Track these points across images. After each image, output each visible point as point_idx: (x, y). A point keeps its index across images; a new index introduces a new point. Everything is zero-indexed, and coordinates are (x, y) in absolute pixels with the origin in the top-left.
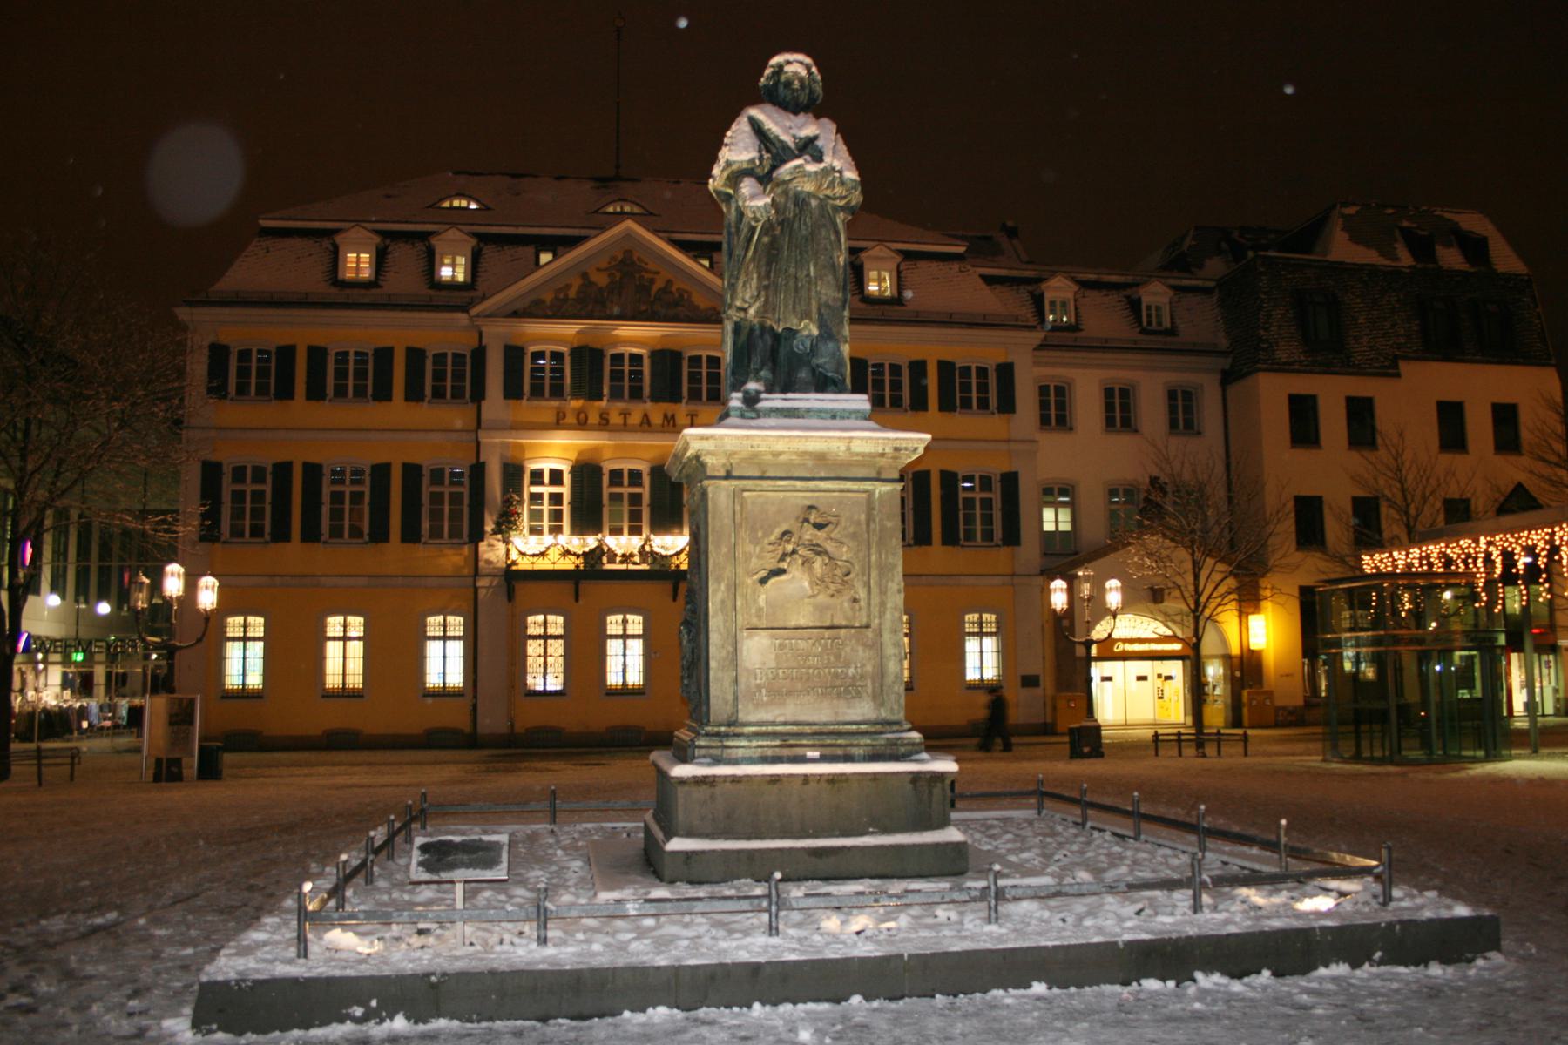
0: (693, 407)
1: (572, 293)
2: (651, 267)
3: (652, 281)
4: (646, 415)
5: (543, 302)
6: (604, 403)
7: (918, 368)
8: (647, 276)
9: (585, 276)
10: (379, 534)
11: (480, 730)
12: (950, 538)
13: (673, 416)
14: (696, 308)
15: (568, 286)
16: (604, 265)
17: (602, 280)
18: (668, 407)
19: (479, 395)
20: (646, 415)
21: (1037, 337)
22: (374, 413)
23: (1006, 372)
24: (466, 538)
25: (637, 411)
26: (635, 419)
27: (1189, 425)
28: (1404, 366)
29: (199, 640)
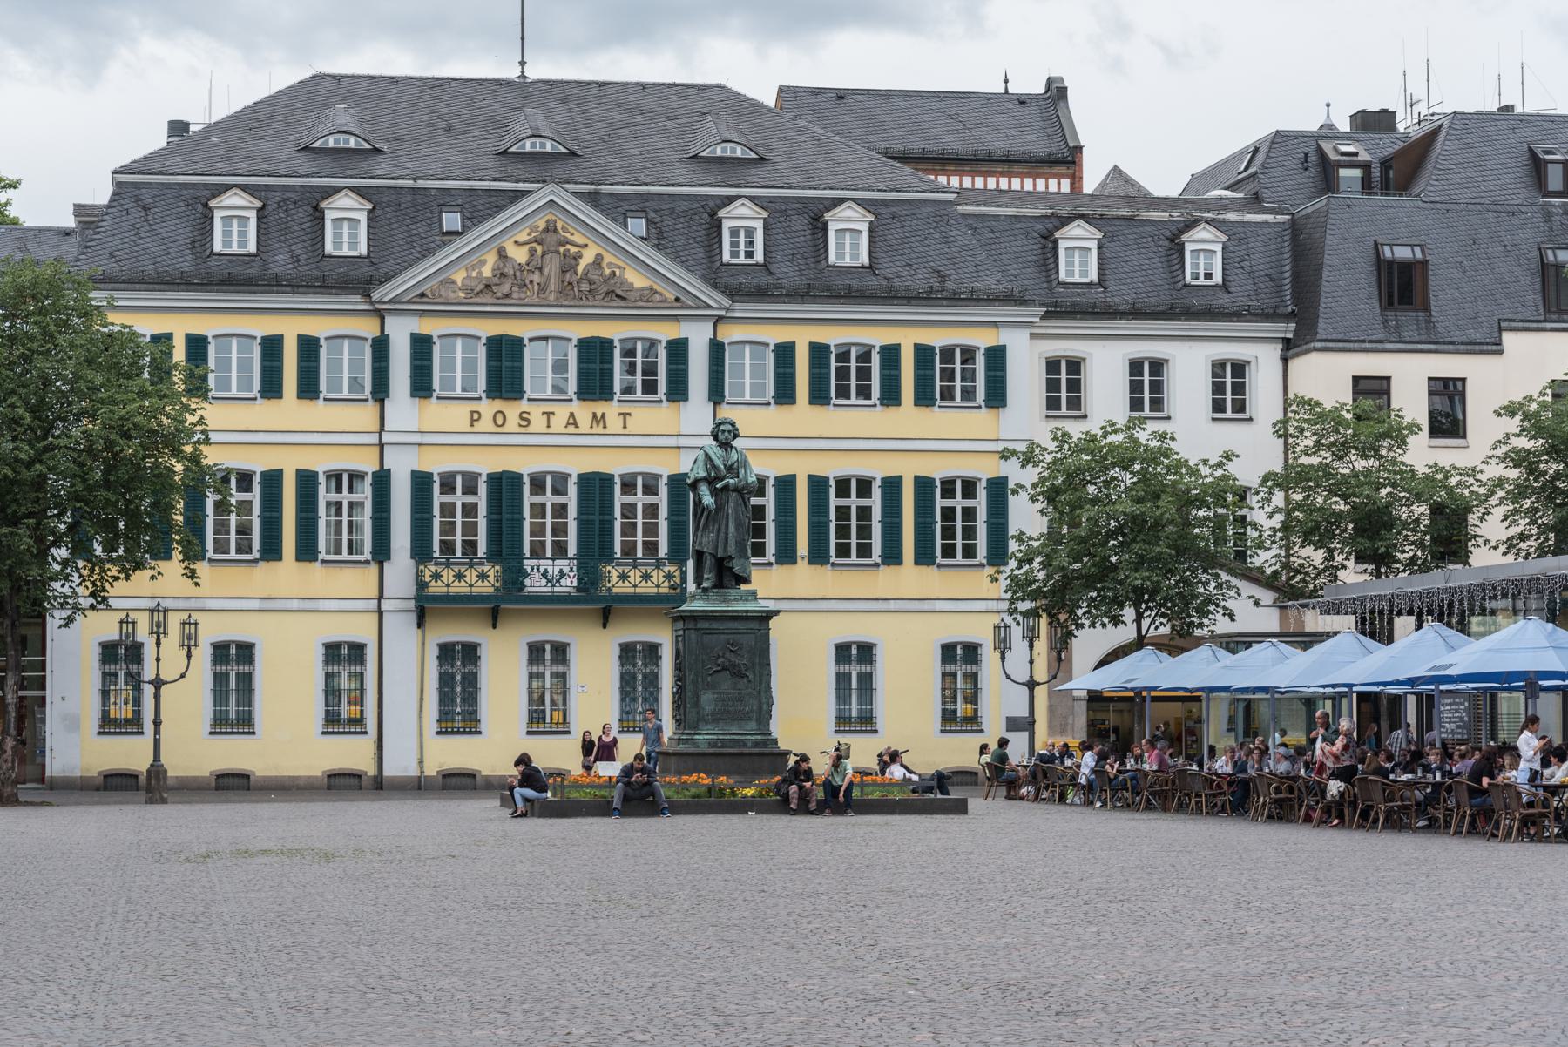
0: (626, 408)
1: (487, 271)
4: (572, 414)
5: (454, 282)
6: (524, 405)
7: (891, 354)
8: (573, 249)
9: (502, 254)
10: (271, 550)
11: (387, 772)
12: (924, 556)
13: (603, 415)
14: (631, 288)
15: (483, 262)
16: (523, 237)
17: (520, 255)
18: (600, 407)
19: (381, 390)
20: (572, 414)
21: (1034, 314)
22: (266, 414)
23: (996, 357)
24: (367, 555)
25: (561, 413)
26: (559, 422)
27: (1240, 407)
28: (1508, 339)
29: (183, 676)
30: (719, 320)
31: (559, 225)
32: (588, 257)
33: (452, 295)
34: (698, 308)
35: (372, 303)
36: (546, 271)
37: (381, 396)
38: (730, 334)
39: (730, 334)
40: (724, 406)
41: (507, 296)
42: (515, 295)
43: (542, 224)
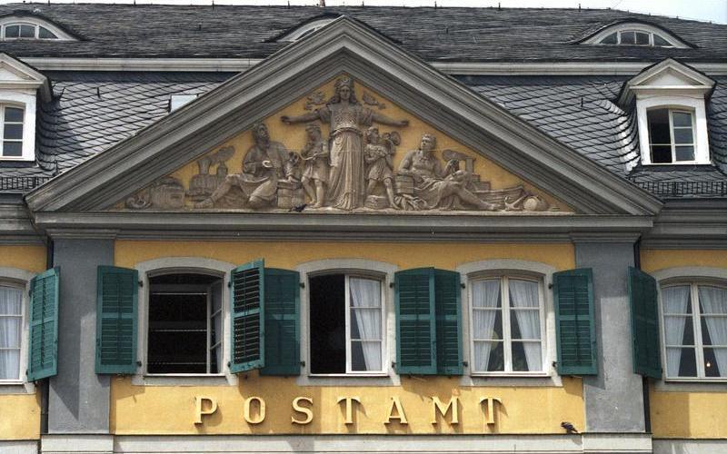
2: (392, 114)
3: (391, 144)
5: (176, 183)
8: (383, 130)
16: (297, 112)
30: (641, 243)
31: (359, 91)
32: (410, 147)
33: (173, 203)
34: (600, 217)
35: (30, 219)
36: (335, 162)
37: (42, 374)
38: (663, 266)
39: (663, 266)
40: (662, 386)
41: (271, 203)
42: (281, 201)
43: (329, 92)
